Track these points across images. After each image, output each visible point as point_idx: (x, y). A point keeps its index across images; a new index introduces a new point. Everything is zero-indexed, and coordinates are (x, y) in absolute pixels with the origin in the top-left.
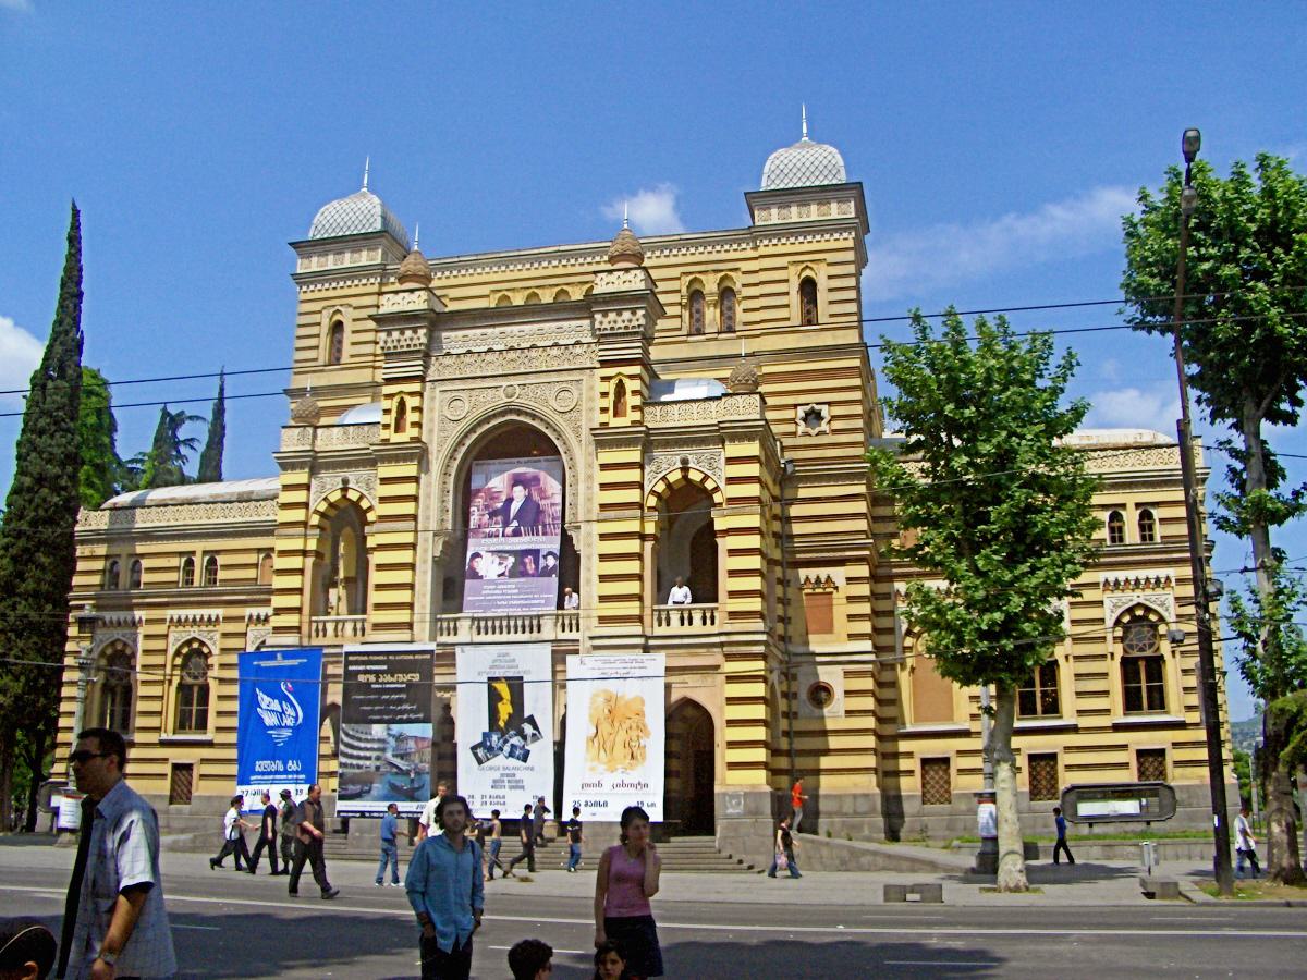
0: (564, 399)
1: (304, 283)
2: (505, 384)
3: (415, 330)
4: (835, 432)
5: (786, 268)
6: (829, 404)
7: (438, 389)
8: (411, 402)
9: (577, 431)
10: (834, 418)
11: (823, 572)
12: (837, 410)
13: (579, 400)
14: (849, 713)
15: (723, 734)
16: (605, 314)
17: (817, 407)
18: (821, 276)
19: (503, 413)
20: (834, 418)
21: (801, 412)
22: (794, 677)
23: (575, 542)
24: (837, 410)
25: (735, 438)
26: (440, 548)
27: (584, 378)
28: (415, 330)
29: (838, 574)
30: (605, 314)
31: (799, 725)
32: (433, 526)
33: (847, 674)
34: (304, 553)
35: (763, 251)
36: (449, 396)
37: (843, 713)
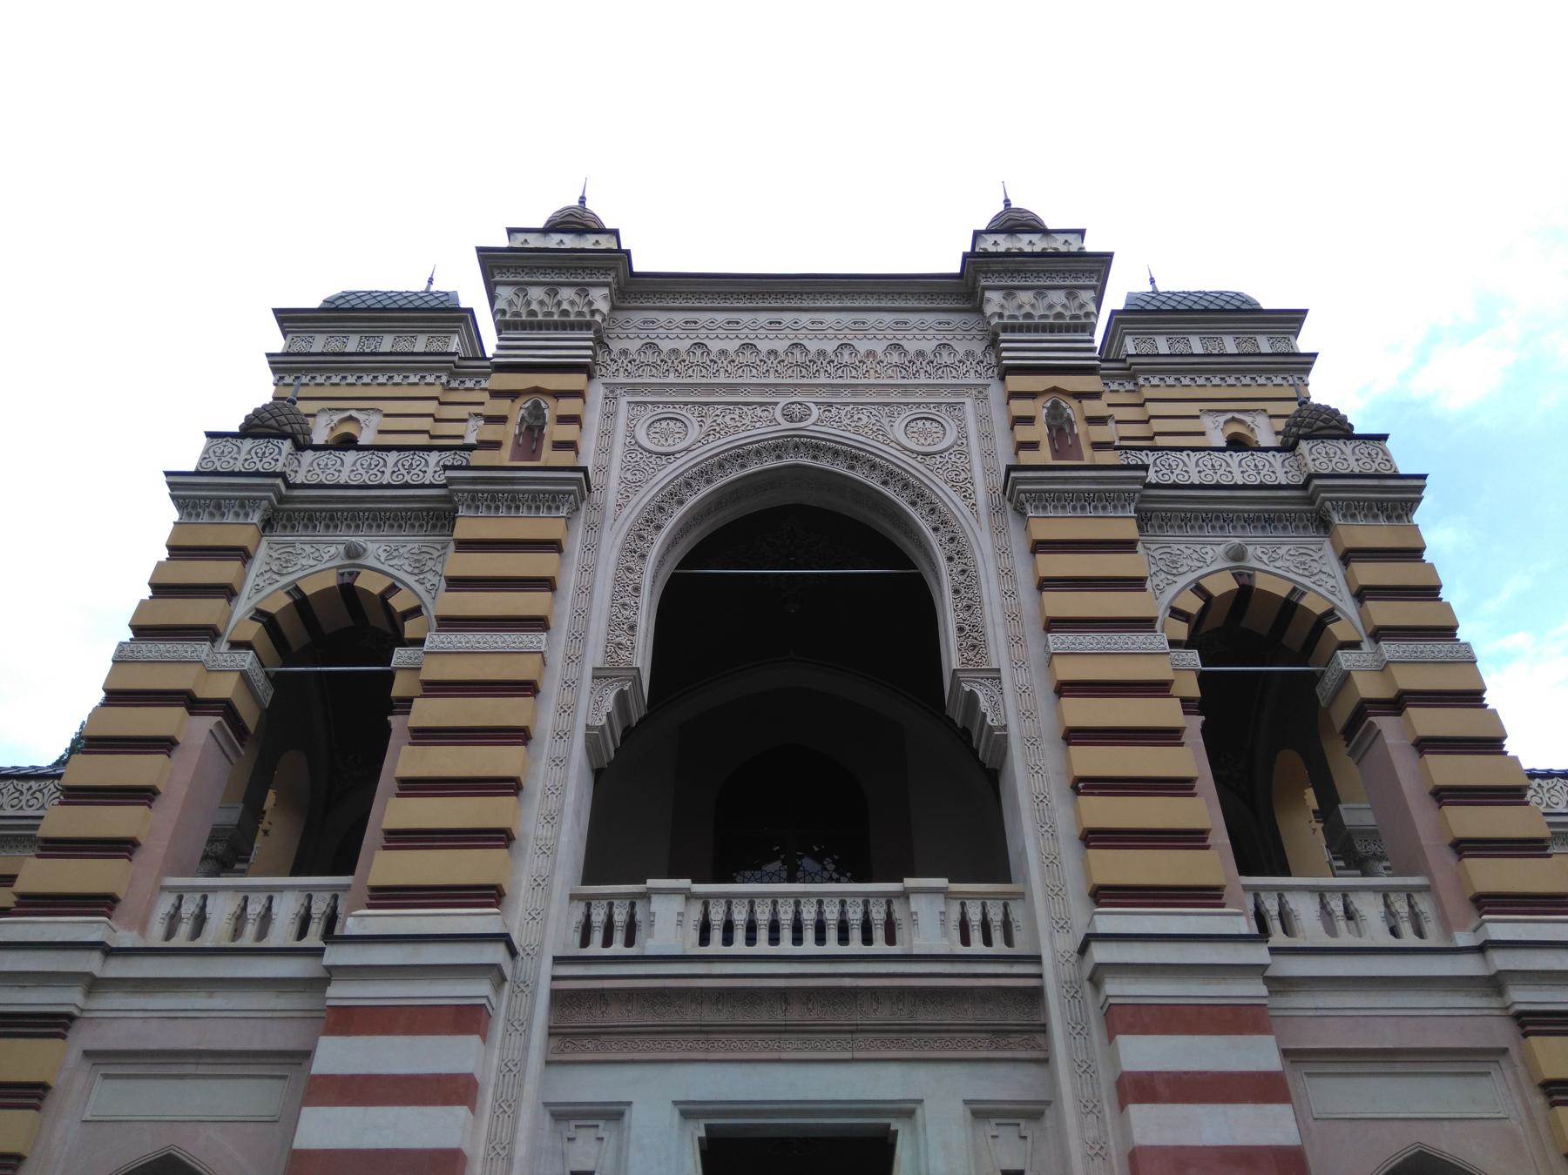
0: (925, 434)
1: (289, 371)
2: (783, 401)
3: (583, 289)
5: (1197, 417)
7: (623, 401)
8: (552, 408)
9: (964, 487)
13: (963, 434)
16: (1010, 291)
19: (778, 448)
23: (984, 704)
25: (1352, 510)
26: (609, 704)
27: (969, 402)
28: (583, 289)
30: (1010, 291)
32: (595, 656)
34: (193, 703)
35: (1148, 393)
36: (648, 414)
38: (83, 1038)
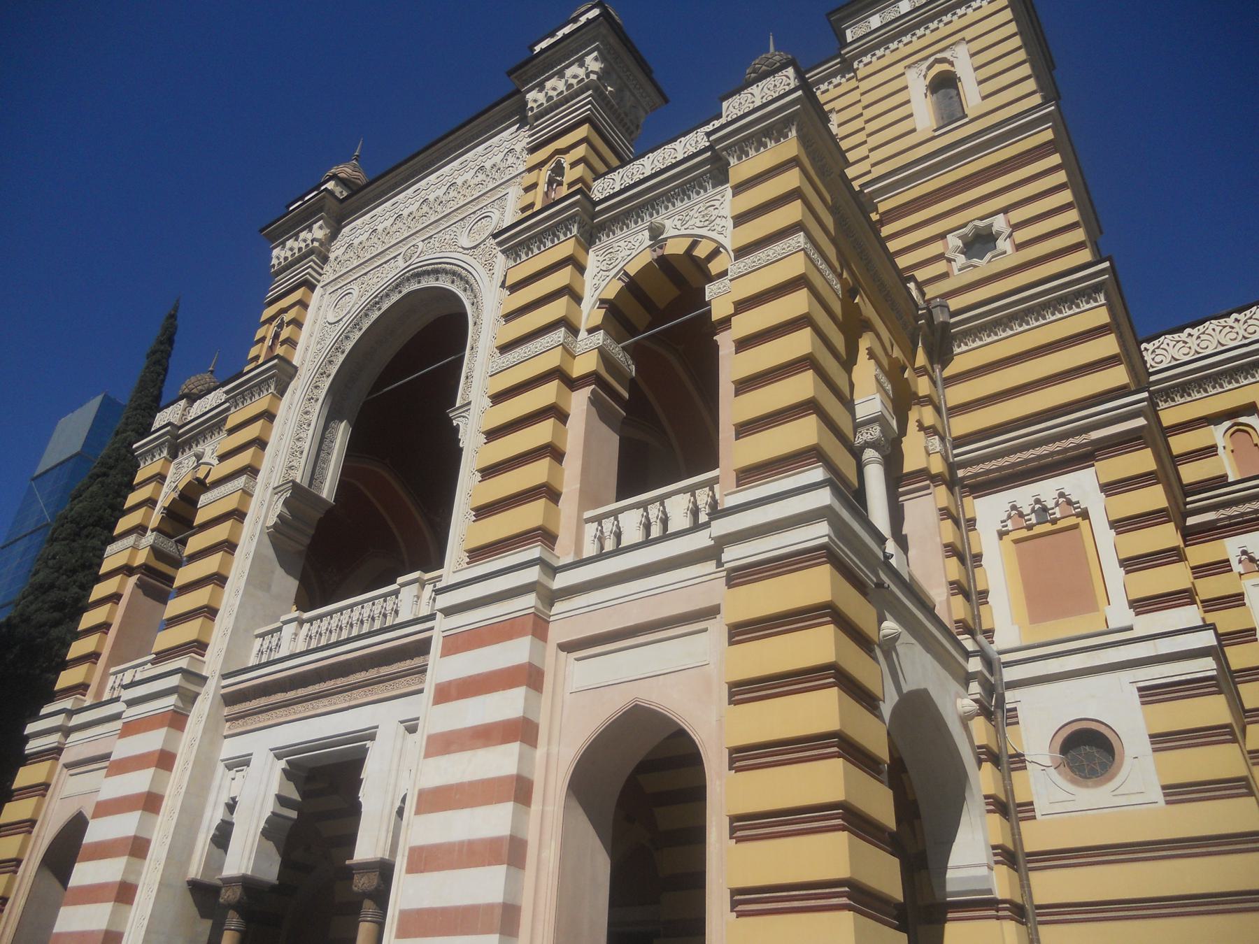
4: (1019, 247)
6: (1005, 210)
10: (1016, 227)
11: (1047, 489)
12: (1017, 216)
14: (1177, 792)
15: (726, 793)
17: (981, 224)
18: (963, 66)
20: (1016, 227)
21: (954, 241)
22: (1012, 717)
24: (1017, 216)
29: (1082, 485)
31: (1034, 838)
33: (1149, 694)
37: (1158, 795)
38: (66, 757)
